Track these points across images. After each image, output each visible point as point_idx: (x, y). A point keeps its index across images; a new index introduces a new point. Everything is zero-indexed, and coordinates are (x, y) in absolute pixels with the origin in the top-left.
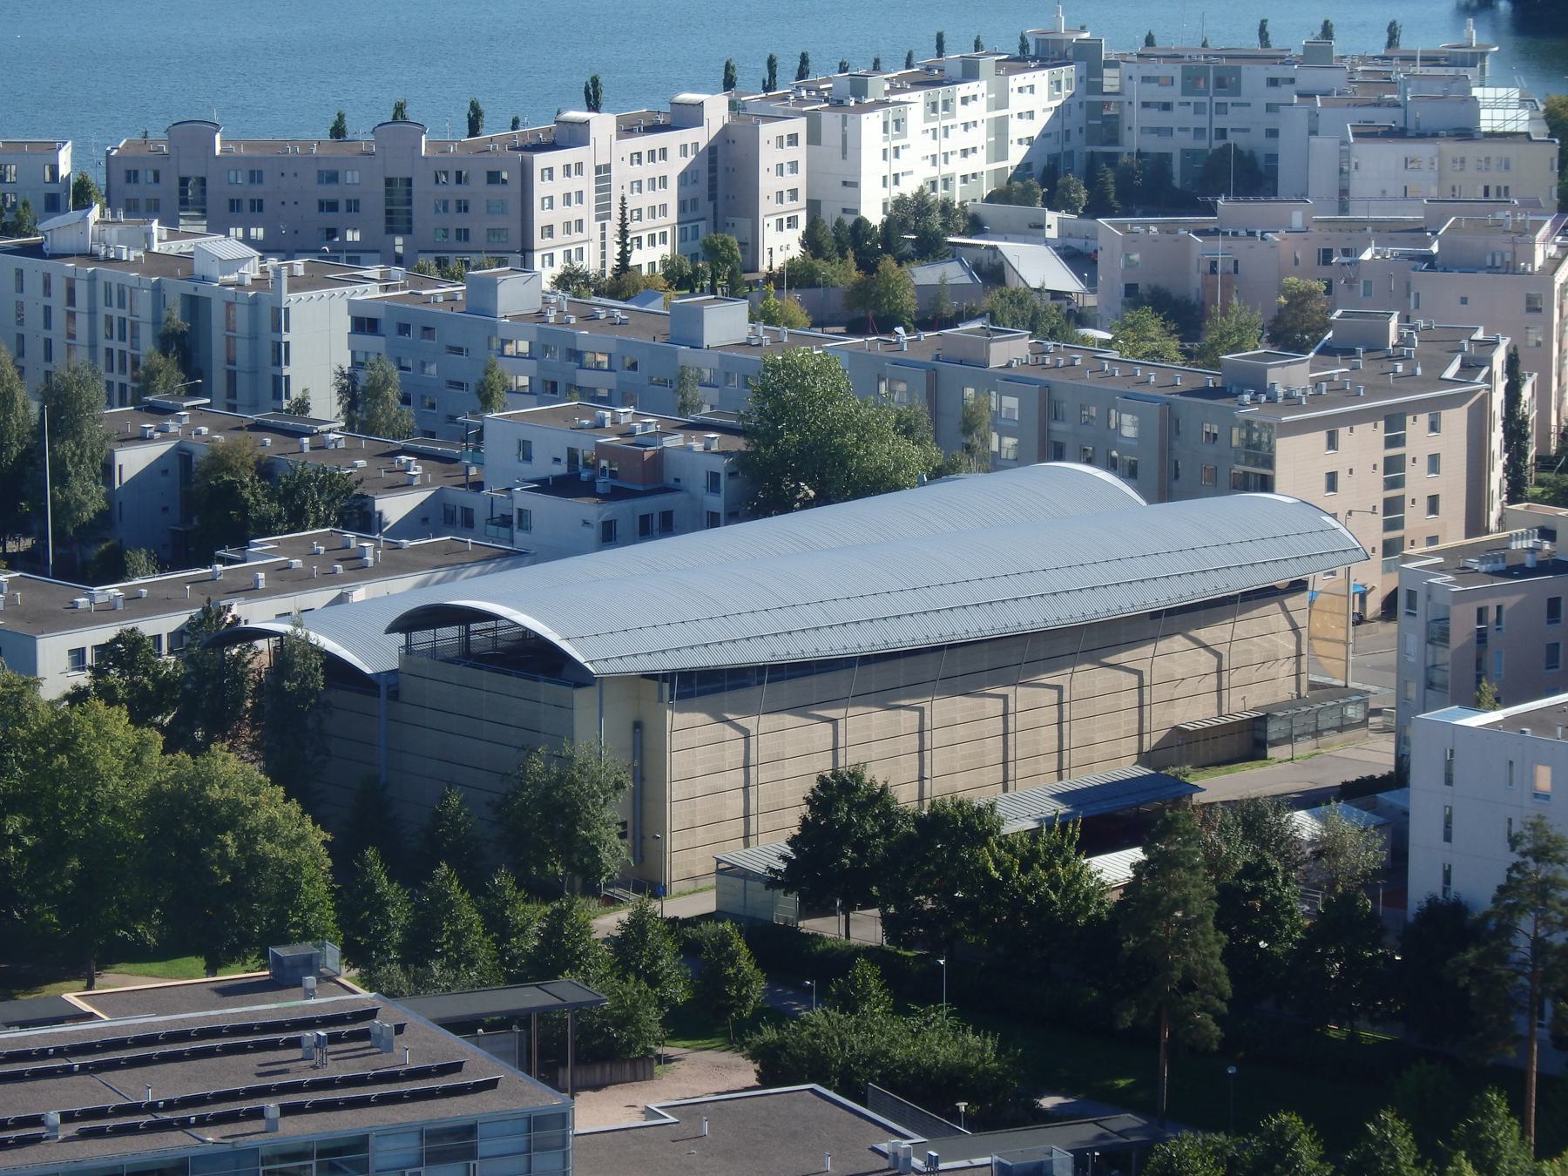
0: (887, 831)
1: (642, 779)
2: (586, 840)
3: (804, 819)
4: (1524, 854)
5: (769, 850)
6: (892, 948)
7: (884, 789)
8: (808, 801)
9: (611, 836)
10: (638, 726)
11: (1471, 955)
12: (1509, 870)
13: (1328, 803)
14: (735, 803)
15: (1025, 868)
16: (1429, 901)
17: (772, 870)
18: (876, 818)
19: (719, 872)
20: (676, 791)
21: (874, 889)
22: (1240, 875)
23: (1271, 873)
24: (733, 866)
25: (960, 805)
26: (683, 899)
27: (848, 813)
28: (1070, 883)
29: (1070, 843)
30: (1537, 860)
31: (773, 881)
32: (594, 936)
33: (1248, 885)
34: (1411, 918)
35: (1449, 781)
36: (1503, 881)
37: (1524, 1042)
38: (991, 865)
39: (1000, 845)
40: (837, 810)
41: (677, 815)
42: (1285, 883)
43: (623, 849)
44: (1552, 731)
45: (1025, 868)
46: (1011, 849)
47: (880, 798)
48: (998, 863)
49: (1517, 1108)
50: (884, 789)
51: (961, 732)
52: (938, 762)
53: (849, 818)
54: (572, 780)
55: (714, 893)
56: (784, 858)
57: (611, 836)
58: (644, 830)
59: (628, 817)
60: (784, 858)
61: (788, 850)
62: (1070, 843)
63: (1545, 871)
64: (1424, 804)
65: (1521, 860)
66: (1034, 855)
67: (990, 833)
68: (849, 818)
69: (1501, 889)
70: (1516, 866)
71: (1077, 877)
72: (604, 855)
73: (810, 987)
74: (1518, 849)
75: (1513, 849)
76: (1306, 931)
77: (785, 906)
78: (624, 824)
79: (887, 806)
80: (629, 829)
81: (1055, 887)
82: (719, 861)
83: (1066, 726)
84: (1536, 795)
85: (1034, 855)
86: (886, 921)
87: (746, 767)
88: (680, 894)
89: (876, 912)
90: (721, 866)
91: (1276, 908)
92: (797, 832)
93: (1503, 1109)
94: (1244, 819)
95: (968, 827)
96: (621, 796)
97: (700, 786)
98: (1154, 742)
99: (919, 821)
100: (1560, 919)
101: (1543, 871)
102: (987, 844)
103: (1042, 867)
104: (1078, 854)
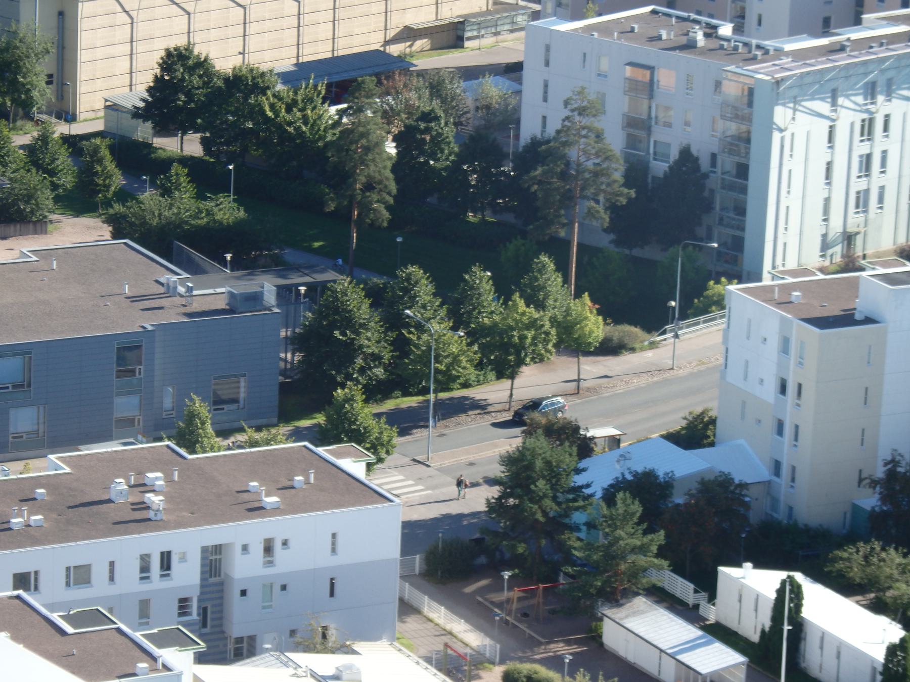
0: (206, 84)
1: (63, 48)
2: (24, 85)
3: (156, 76)
4: (573, 110)
5: (136, 94)
6: (207, 158)
7: (206, 59)
8: (160, 65)
9: (41, 82)
10: (61, 14)
11: (539, 171)
12: (564, 120)
13: (484, 76)
14: (125, 64)
15: (289, 110)
16: (532, 139)
17: (135, 107)
18: (200, 76)
19: (106, 107)
20: (83, 56)
21: (199, 121)
22: (418, 120)
23: (437, 118)
24: (115, 105)
25: (252, 70)
26: (86, 123)
27: (182, 74)
28: (315, 121)
29: (318, 96)
30: (580, 114)
31: (137, 114)
32: (13, 144)
33: (422, 125)
34: (521, 149)
35: (547, 64)
36: (559, 127)
37: (570, 225)
38: (267, 108)
39: (274, 96)
40: (176, 71)
41: (84, 71)
42: (446, 124)
43: (48, 91)
44: (611, 35)
45: (289, 110)
46: (280, 99)
47: (203, 65)
48: (272, 107)
49: (562, 267)
50: (206, 59)
51: (268, 25)
52: (253, 43)
53: (183, 76)
54: (17, 47)
55: (102, 121)
56: (144, 100)
57: (41, 82)
58: (63, 79)
59: (53, 70)
60: (144, 100)
61: (146, 95)
62: (318, 96)
63: (585, 121)
64: (532, 79)
65: (570, 114)
66: (295, 102)
67: (268, 88)
68: (183, 76)
69: (558, 132)
70: (567, 118)
71: (320, 117)
72: (35, 94)
73: (146, 180)
74: (569, 107)
75: (566, 107)
76: (457, 155)
77: (143, 131)
78: (50, 76)
79: (208, 69)
80: (55, 79)
81: (306, 123)
82: (106, 100)
83: (336, 22)
84: (599, 75)
85: (295, 102)
86: (204, 142)
87: (132, 42)
88: (85, 120)
89: (199, 135)
90: (108, 103)
91: (438, 141)
92: (152, 84)
93: (552, 266)
94: (430, 84)
95: (255, 85)
96: (47, 58)
97: (99, 53)
98: (392, 35)
99: (227, 80)
100: (593, 151)
101: (584, 121)
102: (265, 94)
103: (300, 110)
104: (323, 103)
